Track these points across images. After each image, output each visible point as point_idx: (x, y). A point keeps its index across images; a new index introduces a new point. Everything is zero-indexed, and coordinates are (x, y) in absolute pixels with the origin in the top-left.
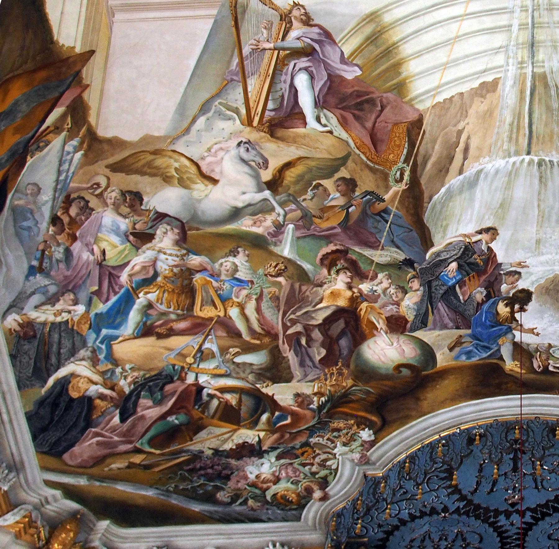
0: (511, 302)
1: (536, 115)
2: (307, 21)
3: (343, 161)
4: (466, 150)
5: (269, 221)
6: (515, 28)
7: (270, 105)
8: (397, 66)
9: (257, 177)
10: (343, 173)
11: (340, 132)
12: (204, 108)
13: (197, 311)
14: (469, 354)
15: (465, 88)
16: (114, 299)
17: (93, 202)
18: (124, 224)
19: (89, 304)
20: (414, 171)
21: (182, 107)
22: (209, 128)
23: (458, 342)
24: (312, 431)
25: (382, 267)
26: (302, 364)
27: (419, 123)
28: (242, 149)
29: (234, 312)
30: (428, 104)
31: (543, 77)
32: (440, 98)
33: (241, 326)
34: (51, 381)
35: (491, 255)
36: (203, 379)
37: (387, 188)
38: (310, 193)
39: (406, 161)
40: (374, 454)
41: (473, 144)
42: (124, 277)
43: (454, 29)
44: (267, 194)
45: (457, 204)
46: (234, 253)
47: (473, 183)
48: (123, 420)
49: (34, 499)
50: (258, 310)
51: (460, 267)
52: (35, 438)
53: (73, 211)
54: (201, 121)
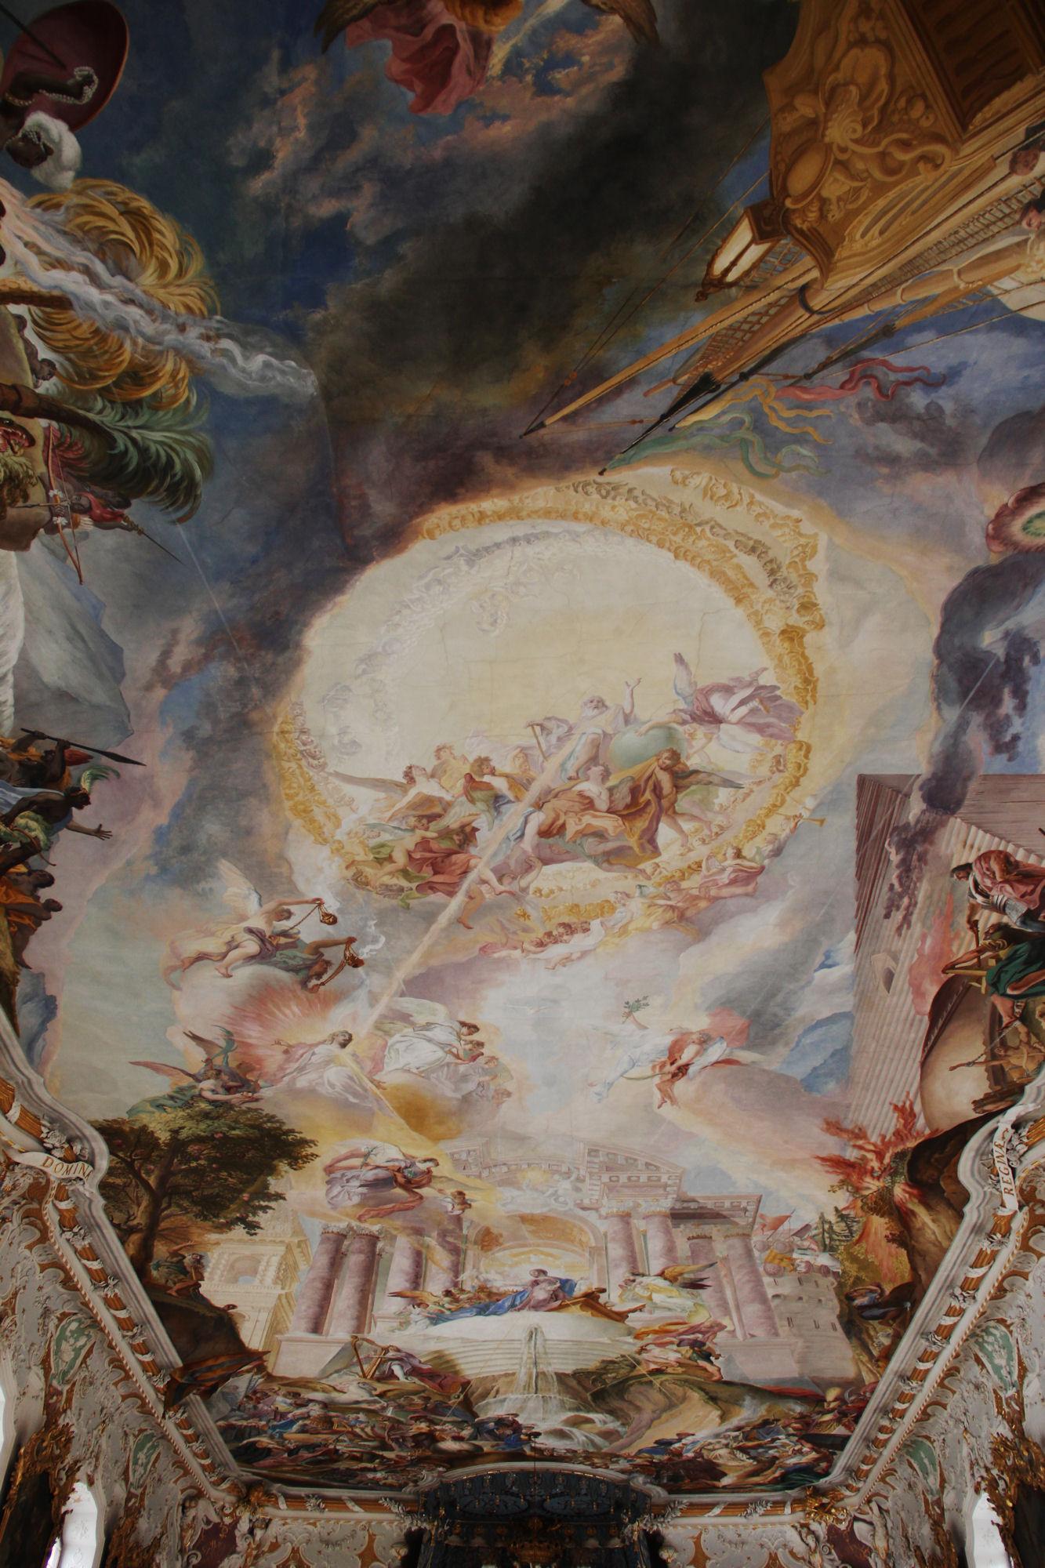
1: (540, 1382)
2: (398, 1350)
3: (423, 1391)
4: (497, 1392)
5: (378, 1406)
6: (525, 1358)
8: (454, 1366)
11: (418, 1382)
12: (337, 1371)
13: (335, 1427)
18: (289, 1401)
19: (269, 1421)
20: (466, 1396)
21: (324, 1370)
22: (340, 1377)
23: (497, 1445)
24: (407, 1466)
29: (358, 1430)
31: (544, 1373)
35: (515, 1422)
40: (447, 1475)
41: (501, 1391)
42: (290, 1416)
43: (487, 1357)
47: (505, 1400)
49: (235, 1475)
50: (373, 1428)
52: (235, 1457)
54: (335, 1375)
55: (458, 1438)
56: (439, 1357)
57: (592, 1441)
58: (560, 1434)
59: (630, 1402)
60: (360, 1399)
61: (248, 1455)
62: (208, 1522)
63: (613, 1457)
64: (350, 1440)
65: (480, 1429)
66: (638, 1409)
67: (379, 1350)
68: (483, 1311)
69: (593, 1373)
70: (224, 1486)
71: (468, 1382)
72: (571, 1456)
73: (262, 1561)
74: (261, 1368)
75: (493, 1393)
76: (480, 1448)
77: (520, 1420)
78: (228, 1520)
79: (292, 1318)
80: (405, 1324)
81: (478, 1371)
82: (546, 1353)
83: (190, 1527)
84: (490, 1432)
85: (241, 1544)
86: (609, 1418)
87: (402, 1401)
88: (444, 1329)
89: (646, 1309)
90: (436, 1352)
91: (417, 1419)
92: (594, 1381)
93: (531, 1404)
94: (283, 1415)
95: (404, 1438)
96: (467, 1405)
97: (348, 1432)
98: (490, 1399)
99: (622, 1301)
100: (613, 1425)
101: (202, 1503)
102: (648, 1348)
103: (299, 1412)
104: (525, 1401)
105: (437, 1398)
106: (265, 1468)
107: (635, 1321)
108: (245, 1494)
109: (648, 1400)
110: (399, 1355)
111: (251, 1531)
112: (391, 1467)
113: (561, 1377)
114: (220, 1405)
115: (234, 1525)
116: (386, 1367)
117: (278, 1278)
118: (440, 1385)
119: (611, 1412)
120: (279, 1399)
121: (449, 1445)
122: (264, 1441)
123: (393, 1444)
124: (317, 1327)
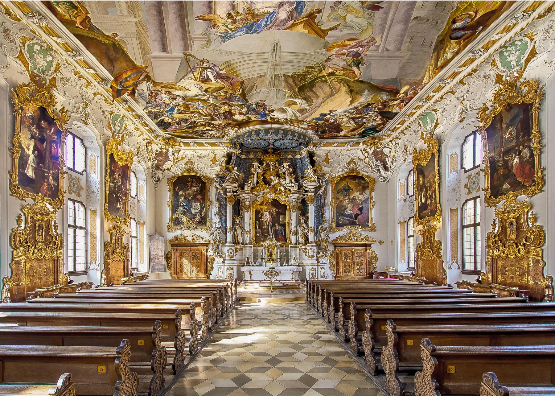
0: (269, 111)
2: (208, 62)
3: (224, 88)
4: (257, 87)
6: (270, 65)
7: (201, 78)
9: (201, 90)
10: (223, 90)
12: (183, 78)
13: (191, 110)
14: (259, 118)
15: (255, 76)
16: (170, 108)
17: (158, 93)
18: (168, 97)
21: (177, 77)
23: (257, 117)
25: (236, 105)
26: (219, 119)
27: (243, 82)
28: (195, 85)
29: (201, 111)
30: (246, 78)
32: (249, 78)
33: (202, 113)
34: (159, 120)
35: (264, 104)
36: (195, 120)
37: (236, 93)
38: (215, 93)
39: (241, 88)
42: (171, 105)
43: (252, 65)
44: (204, 93)
45: (255, 96)
46: (198, 102)
48: (178, 125)
51: (256, 106)
53: (154, 94)
54: (183, 80)
55: (241, 114)
56: (228, 64)
57: (294, 114)
58: (283, 111)
59: (315, 93)
60: (197, 94)
61: (163, 125)
62: (157, 151)
63: (301, 122)
64: (199, 116)
65: (249, 107)
66: (317, 96)
67: (199, 63)
68: (250, 29)
69: (301, 75)
70: (159, 139)
71: (243, 82)
72: (286, 121)
73: (179, 163)
74: (148, 78)
75: (255, 88)
76: (250, 118)
77: (266, 103)
78: (164, 151)
79: (150, 41)
80: (209, 42)
81: (247, 74)
82: (280, 62)
83: (150, 152)
84: (254, 110)
85: (171, 158)
86: (304, 101)
87: (215, 94)
88: (229, 45)
89: (339, 28)
90: (227, 62)
91: (223, 104)
92: (302, 79)
93: (271, 94)
94: (168, 104)
95: (219, 114)
96: (243, 95)
97: (197, 112)
98: (253, 92)
99: (329, 20)
100: (305, 105)
101: (152, 145)
102: (331, 58)
103: (174, 102)
104: (269, 92)
105: (230, 92)
106: (171, 131)
107: (330, 38)
108: (168, 141)
109: (322, 91)
110: (210, 65)
111: (174, 154)
112: (218, 128)
113: (286, 77)
114: (141, 101)
115: (167, 151)
116: (204, 74)
117: (128, 7)
118: (231, 84)
119: (305, 99)
120: (164, 95)
121: (238, 117)
122: (166, 118)
123: (216, 117)
124: (164, 49)
